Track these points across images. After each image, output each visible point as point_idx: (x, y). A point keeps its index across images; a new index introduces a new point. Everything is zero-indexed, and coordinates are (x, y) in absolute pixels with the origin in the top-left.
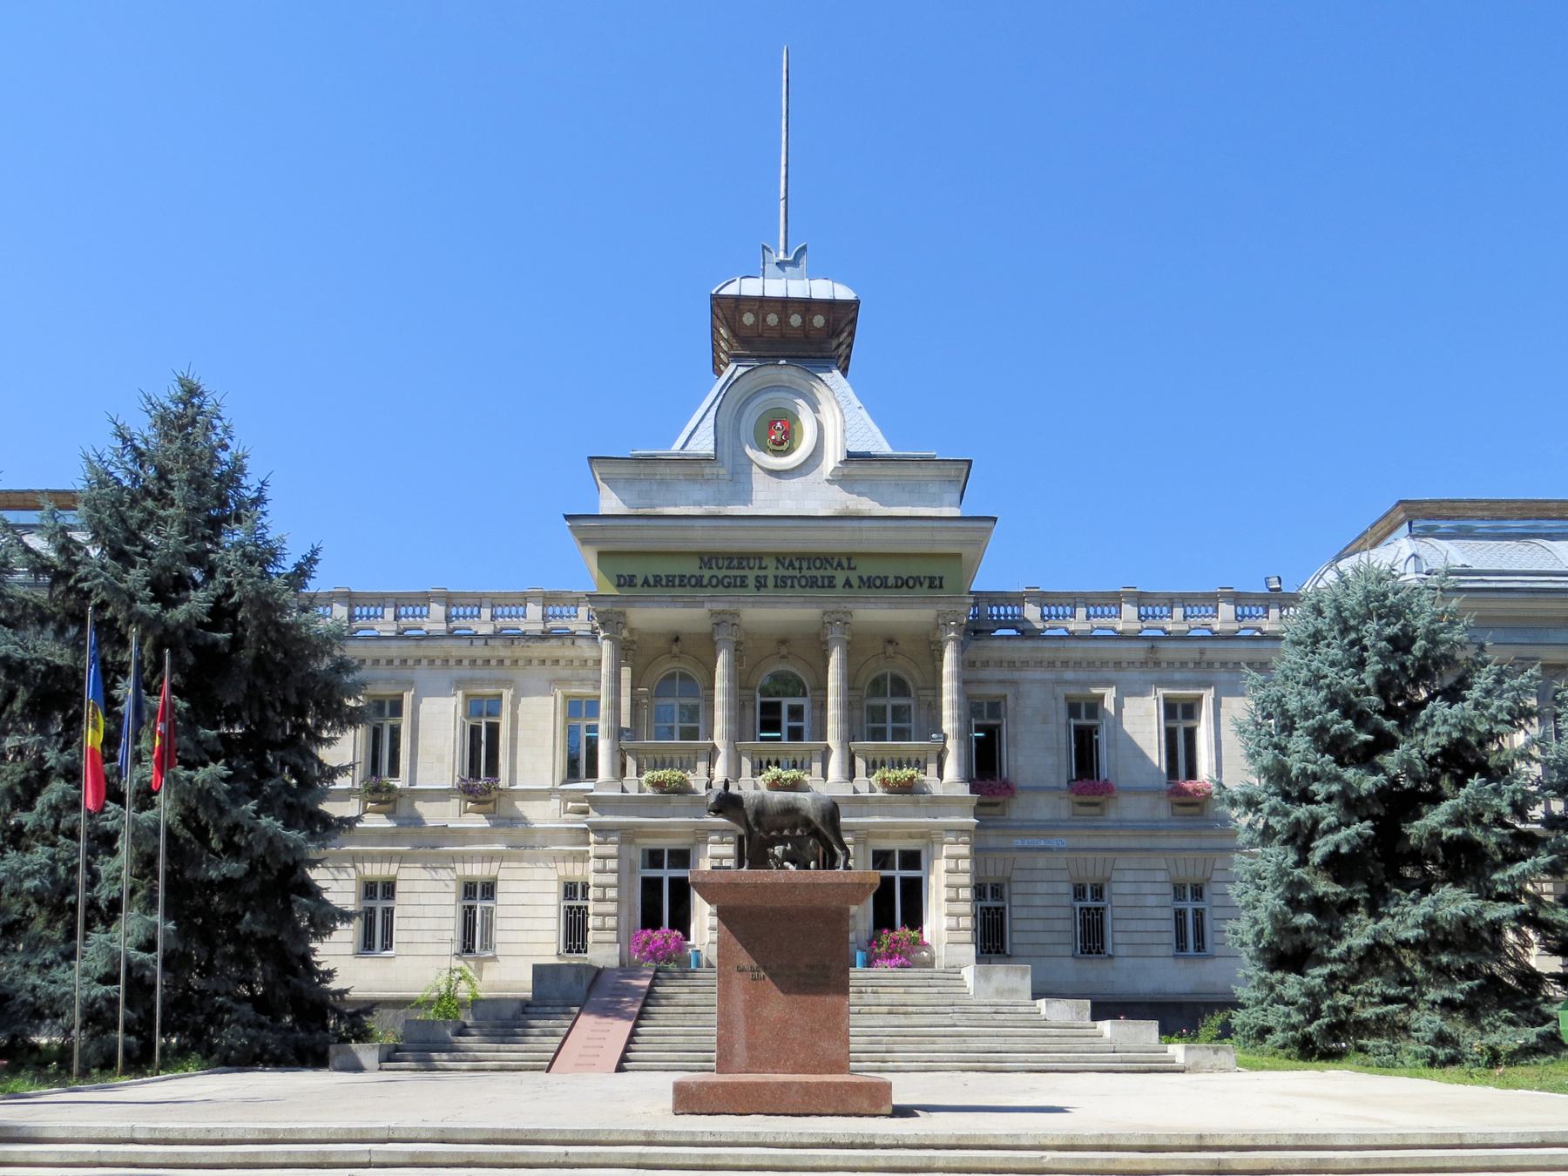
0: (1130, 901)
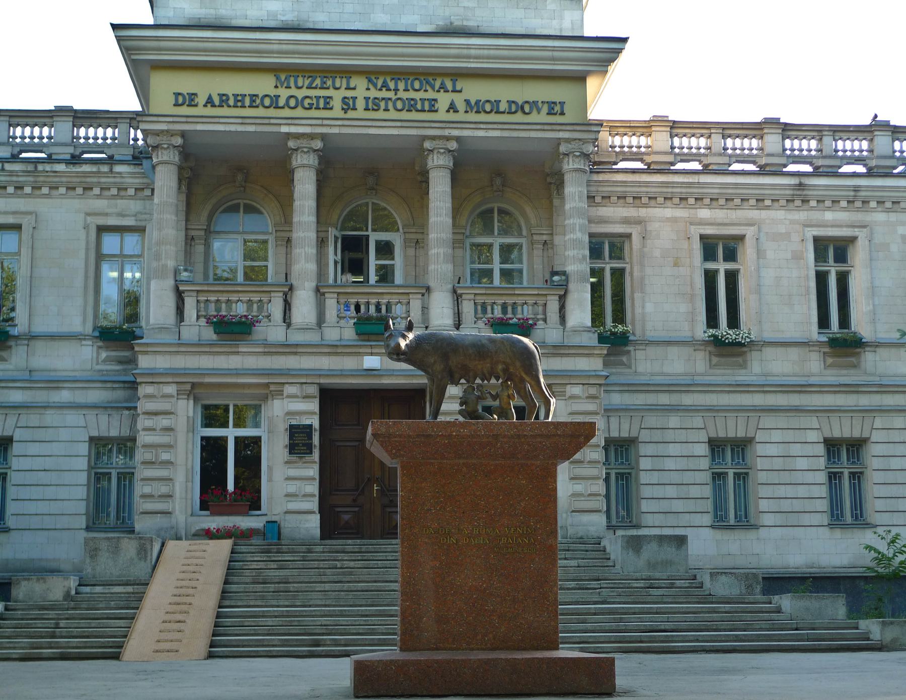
0: (778, 463)
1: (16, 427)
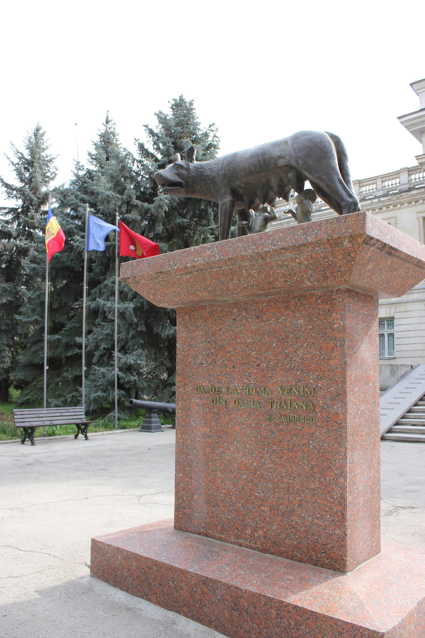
1: (395, 312)
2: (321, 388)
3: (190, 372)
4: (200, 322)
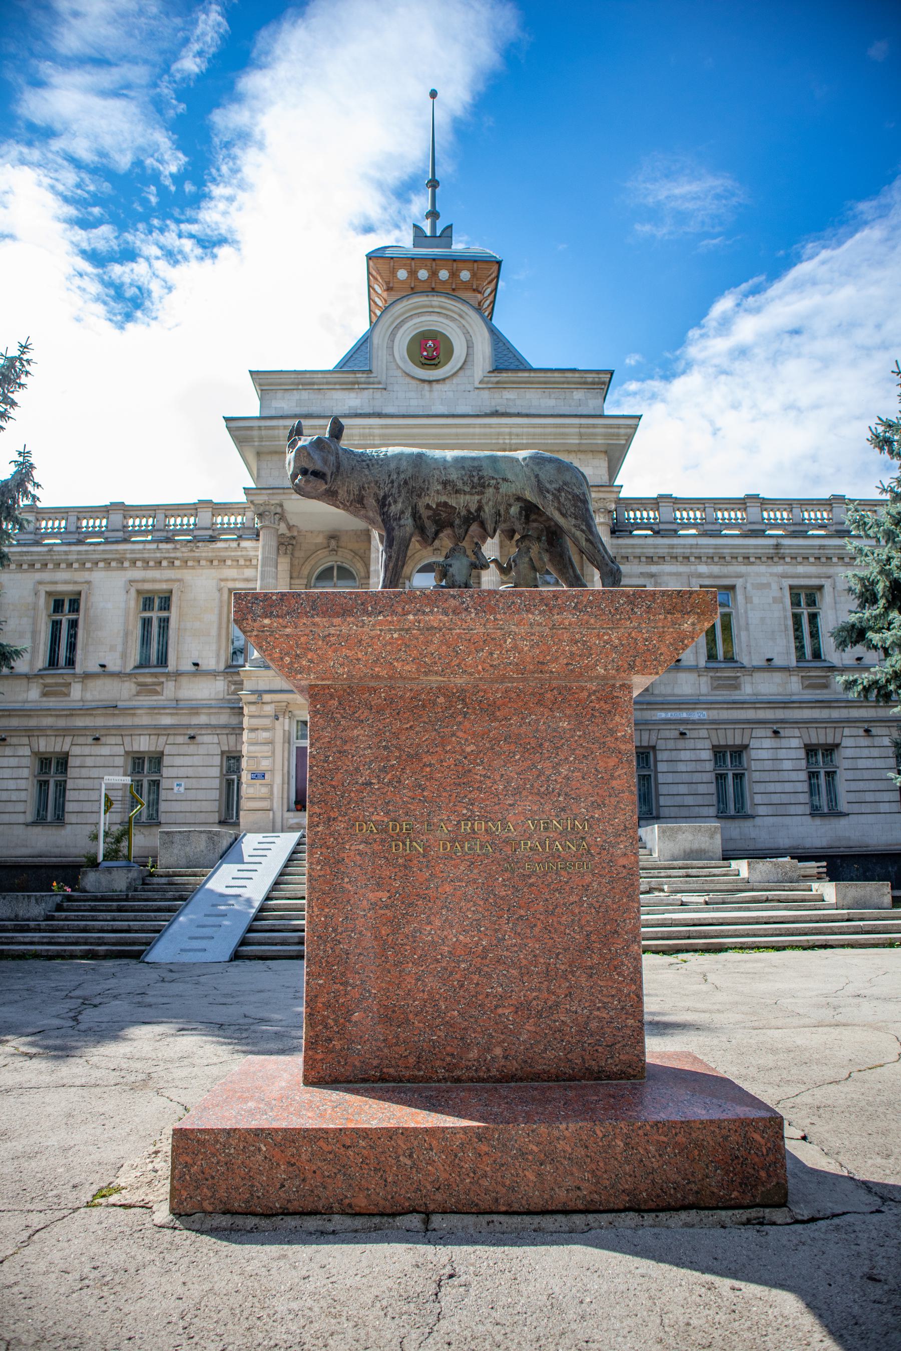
0: (768, 765)
2: (599, 820)
3: (342, 797)
4: (365, 714)
